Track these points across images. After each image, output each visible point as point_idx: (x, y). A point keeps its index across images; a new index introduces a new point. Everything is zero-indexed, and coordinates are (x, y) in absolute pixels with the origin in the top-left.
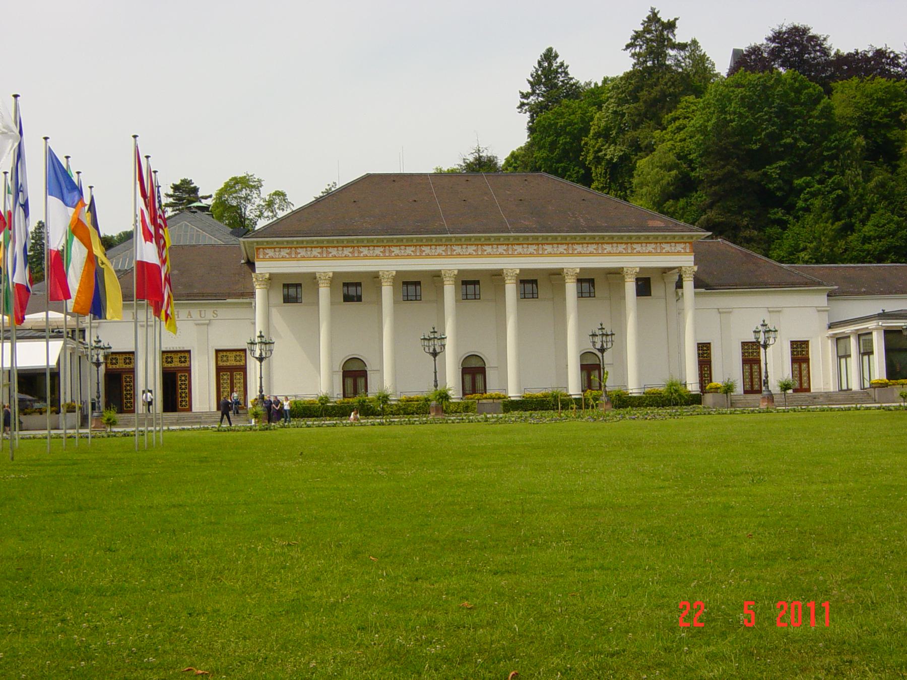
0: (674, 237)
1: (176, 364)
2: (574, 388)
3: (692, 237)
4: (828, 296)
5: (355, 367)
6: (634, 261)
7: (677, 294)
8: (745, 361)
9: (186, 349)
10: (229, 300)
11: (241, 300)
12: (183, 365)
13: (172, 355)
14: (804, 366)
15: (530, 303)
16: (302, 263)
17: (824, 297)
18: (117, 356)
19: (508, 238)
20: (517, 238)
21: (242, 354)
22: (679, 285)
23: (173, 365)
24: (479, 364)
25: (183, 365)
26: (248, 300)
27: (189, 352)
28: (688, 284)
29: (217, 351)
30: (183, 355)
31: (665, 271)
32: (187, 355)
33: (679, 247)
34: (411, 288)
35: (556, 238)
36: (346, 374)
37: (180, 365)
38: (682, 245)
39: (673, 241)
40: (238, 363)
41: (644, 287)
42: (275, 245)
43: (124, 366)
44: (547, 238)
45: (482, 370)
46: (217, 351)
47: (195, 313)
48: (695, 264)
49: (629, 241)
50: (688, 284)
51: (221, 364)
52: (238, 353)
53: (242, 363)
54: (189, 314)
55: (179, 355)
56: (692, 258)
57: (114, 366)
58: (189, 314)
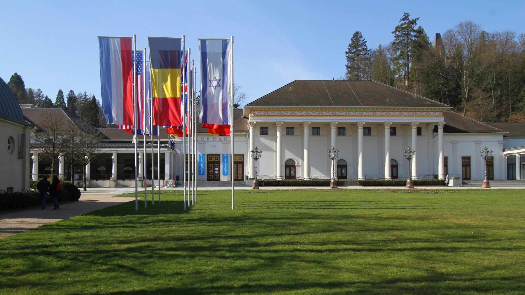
0: (435, 109)
1: (214, 160)
2: (387, 176)
3: (443, 109)
4: (504, 136)
5: (290, 163)
6: (416, 119)
7: (433, 134)
8: (463, 165)
9: (219, 154)
11: (242, 133)
14: (491, 168)
15: (394, 137)
16: (271, 118)
17: (501, 138)
19: (360, 109)
20: (364, 109)
21: (242, 157)
22: (436, 130)
24: (345, 164)
28: (441, 130)
31: (428, 124)
33: (437, 114)
34: (316, 130)
35: (381, 109)
36: (287, 166)
38: (439, 113)
39: (435, 111)
41: (419, 132)
42: (258, 109)
44: (377, 109)
45: (345, 166)
48: (445, 121)
49: (415, 111)
50: (441, 130)
53: (242, 160)
56: (443, 118)
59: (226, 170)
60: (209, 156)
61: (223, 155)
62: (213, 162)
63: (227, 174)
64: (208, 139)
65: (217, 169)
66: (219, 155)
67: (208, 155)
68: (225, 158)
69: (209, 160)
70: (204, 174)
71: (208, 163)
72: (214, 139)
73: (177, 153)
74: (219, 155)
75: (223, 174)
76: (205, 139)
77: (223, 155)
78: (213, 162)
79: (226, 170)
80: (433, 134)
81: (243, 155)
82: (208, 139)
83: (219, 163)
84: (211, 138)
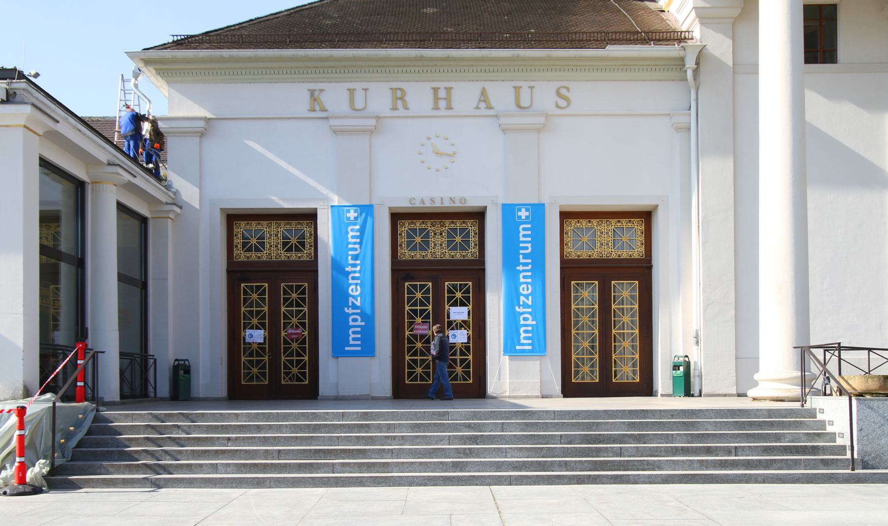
9: (474, 202)
10: (613, 50)
13: (428, 225)
18: (264, 227)
21: (638, 226)
30: (458, 225)
32: (472, 227)
43: (283, 256)
47: (501, 94)
53: (638, 252)
54: (484, 96)
57: (253, 256)
58: (484, 96)
59: (528, 321)
60: (404, 228)
61: (509, 210)
62: (438, 263)
63: (539, 349)
64: (399, 98)
65: (459, 313)
66: (479, 216)
67: (397, 217)
68: (523, 232)
69: (405, 253)
70: (368, 349)
71: (402, 272)
72: (442, 101)
73: (176, 202)
74: (479, 216)
75: (511, 348)
76: (378, 96)
77: (509, 210)
78: (438, 263)
79: (528, 321)
81: (646, 216)
82: (399, 98)
83: (474, 272)
84: (419, 94)
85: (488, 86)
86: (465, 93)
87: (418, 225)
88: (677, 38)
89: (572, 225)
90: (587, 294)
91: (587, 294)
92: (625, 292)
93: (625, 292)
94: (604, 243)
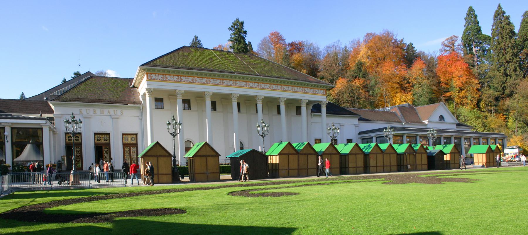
1: (102, 141)
4: (359, 120)
7: (311, 115)
12: (106, 142)
13: (100, 136)
21: (135, 137)
23: (101, 142)
25: (106, 142)
26: (139, 105)
27: (109, 134)
29: (123, 134)
32: (107, 136)
37: (104, 142)
40: (133, 142)
46: (123, 134)
47: (112, 111)
51: (125, 142)
52: (133, 136)
53: (135, 142)
55: (104, 136)
64: (95, 111)
69: (97, 141)
80: (311, 115)
82: (95, 111)
84: (98, 111)
85: (110, 110)
86: (106, 111)
87: (99, 136)
88: (140, 103)
89: (124, 136)
90: (127, 149)
91: (127, 149)
92: (133, 149)
93: (133, 149)
94: (130, 140)
